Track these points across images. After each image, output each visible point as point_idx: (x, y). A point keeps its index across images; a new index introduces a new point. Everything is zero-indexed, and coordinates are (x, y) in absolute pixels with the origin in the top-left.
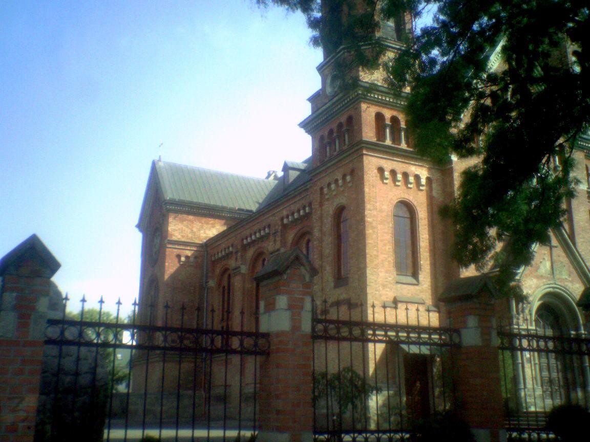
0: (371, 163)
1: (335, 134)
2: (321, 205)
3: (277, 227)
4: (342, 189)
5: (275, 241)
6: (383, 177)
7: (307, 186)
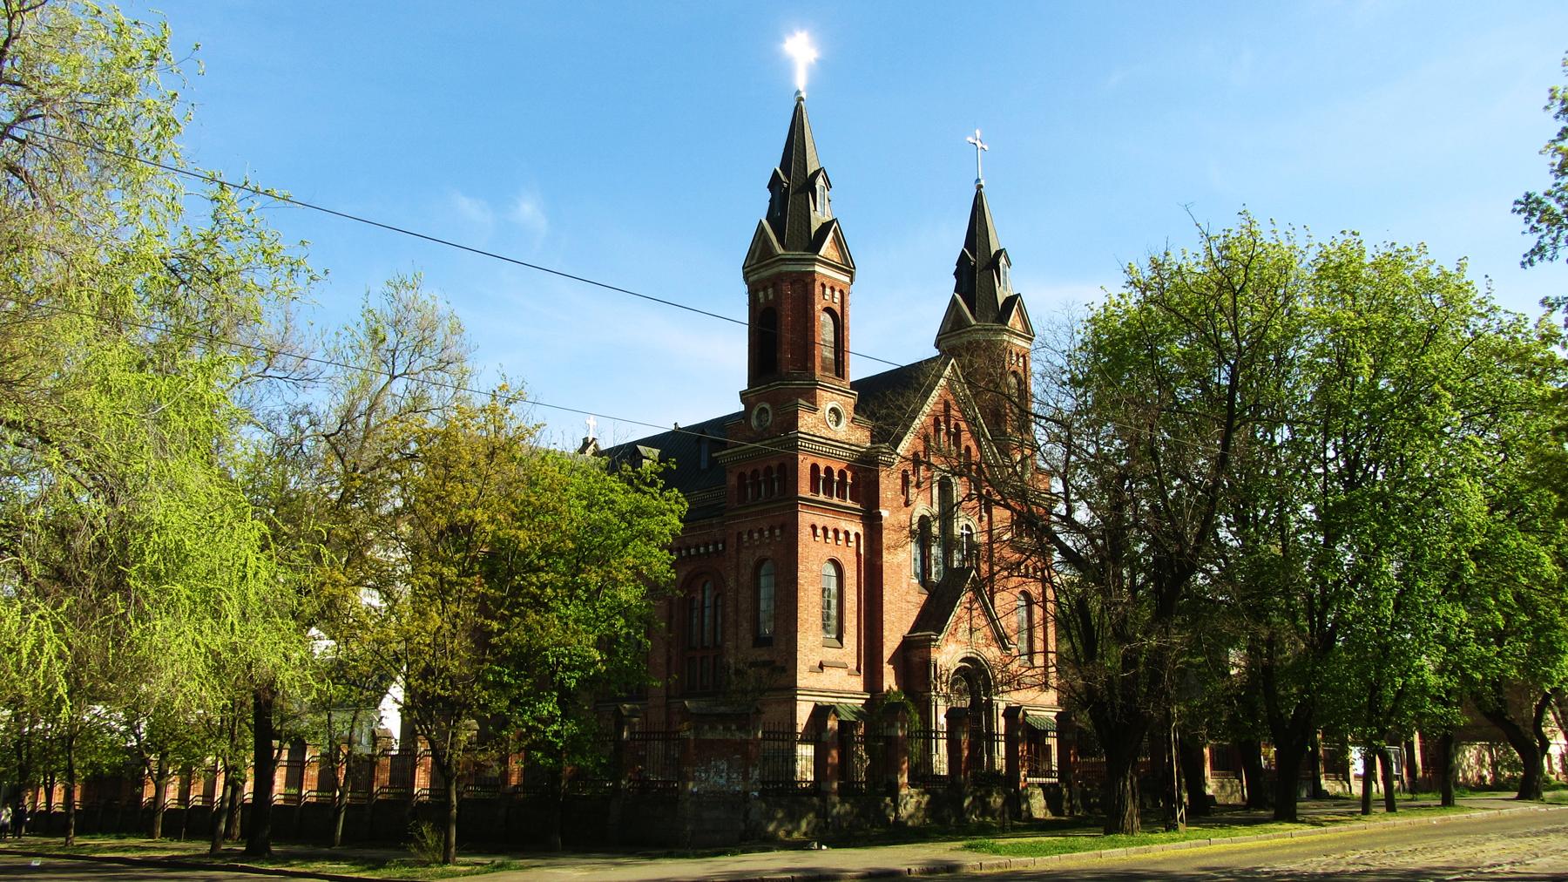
0: (806, 518)
2: (738, 551)
4: (767, 541)
6: (815, 534)
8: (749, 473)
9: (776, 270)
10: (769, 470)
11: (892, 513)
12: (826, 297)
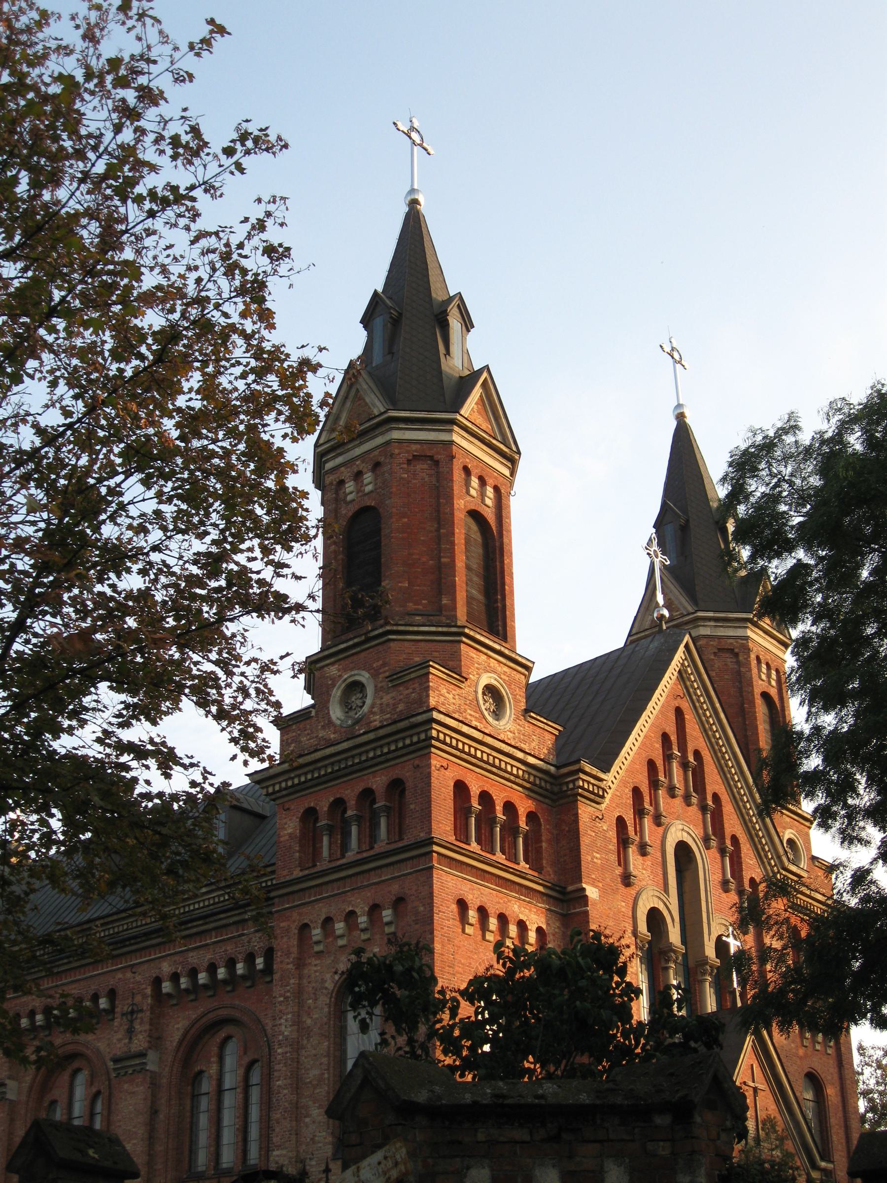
1: (350, 813)
2: (300, 964)
3: (138, 998)
5: (130, 1032)
6: (463, 918)
7: (245, 912)
8: (323, 806)
9: (379, 440)
10: (368, 795)
11: (603, 892)
12: (473, 492)
